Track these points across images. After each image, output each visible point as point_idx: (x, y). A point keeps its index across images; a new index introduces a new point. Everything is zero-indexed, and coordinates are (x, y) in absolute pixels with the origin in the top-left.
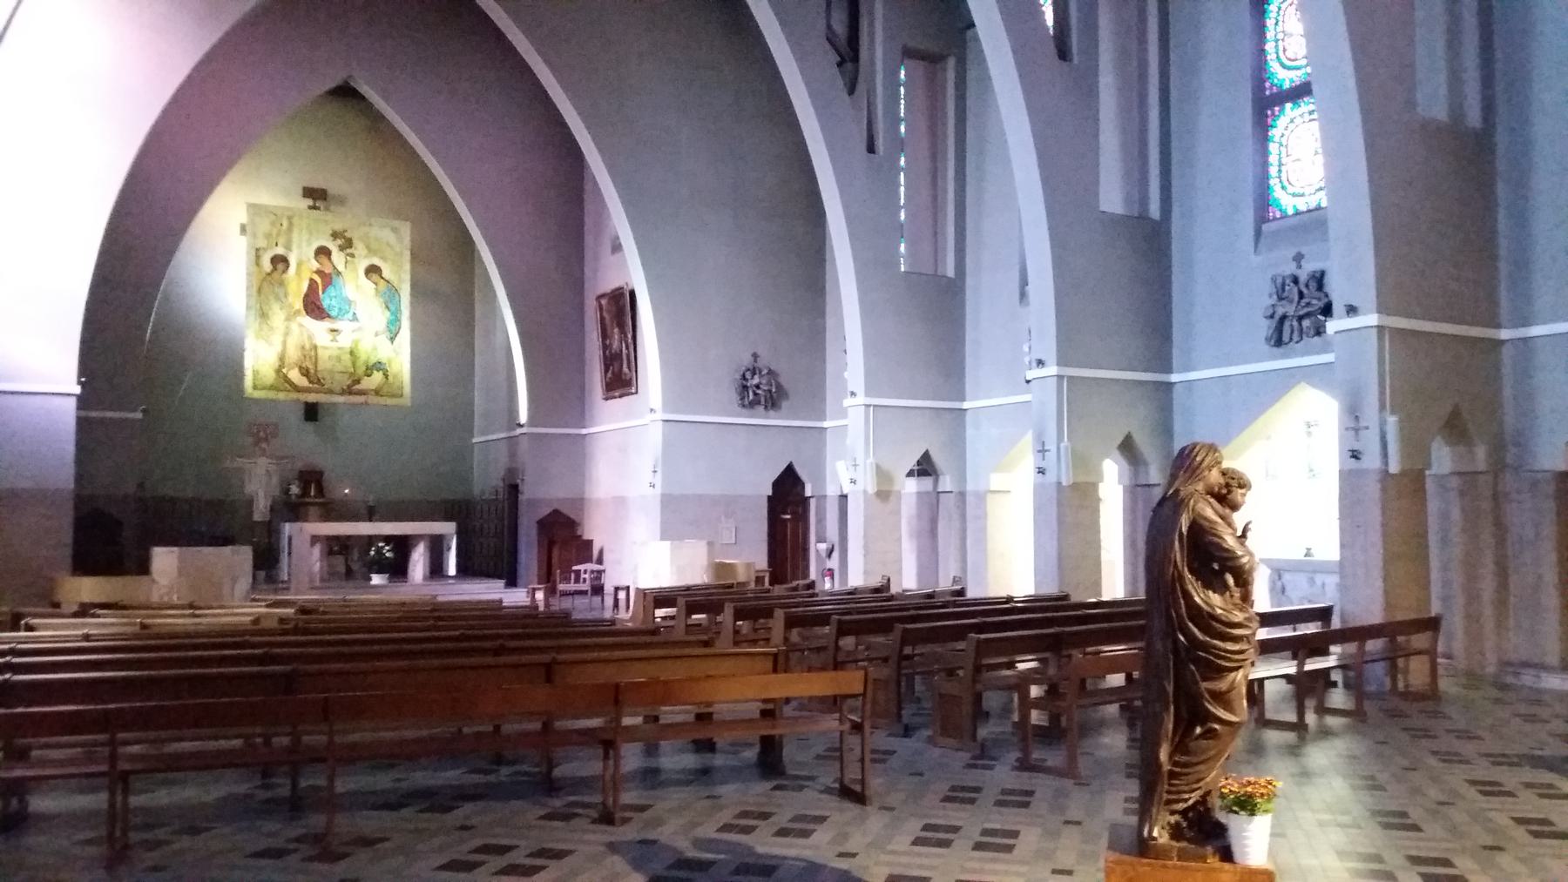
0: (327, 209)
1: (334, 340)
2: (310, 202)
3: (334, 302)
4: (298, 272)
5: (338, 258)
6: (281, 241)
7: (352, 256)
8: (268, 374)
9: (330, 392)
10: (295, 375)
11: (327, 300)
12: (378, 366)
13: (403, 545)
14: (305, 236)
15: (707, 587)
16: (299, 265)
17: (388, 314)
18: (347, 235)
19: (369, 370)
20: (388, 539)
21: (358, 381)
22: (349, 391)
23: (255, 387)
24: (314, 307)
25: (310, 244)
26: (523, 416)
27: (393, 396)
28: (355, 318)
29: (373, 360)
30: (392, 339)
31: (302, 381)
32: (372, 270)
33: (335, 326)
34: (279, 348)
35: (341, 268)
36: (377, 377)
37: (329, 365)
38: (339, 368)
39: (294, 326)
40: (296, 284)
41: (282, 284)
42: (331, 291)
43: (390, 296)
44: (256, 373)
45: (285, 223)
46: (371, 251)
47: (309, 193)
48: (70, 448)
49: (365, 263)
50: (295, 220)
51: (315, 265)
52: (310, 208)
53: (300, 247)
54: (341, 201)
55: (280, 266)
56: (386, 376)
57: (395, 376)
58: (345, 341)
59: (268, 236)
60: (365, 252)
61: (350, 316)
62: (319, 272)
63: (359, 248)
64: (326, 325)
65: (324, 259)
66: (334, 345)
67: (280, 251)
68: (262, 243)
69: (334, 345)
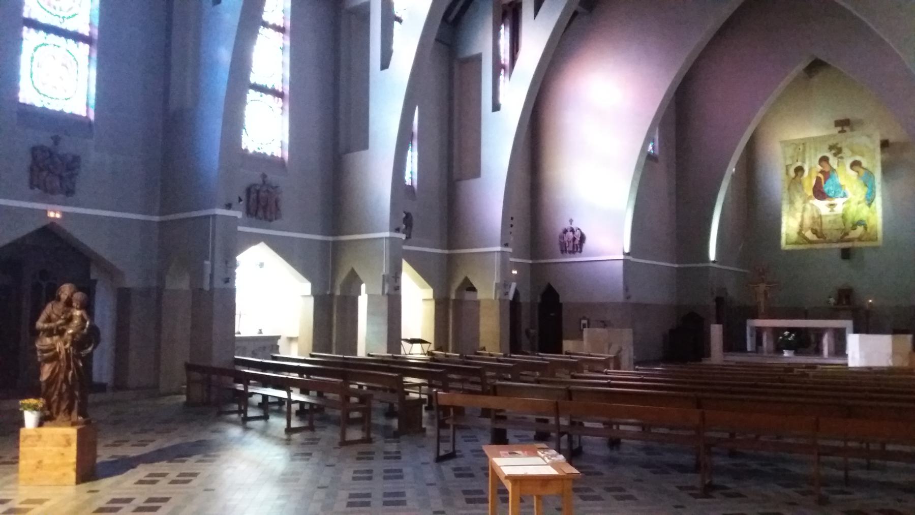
0: (852, 130)
1: (832, 211)
2: (839, 129)
3: (831, 188)
4: (810, 175)
5: (833, 162)
6: (800, 158)
7: (842, 158)
8: (794, 235)
9: (830, 242)
10: (809, 234)
11: (828, 187)
12: (861, 223)
13: (820, 332)
14: (813, 151)
15: (890, 371)
16: (810, 170)
17: (866, 189)
18: (839, 146)
19: (855, 226)
20: (791, 330)
21: (847, 234)
22: (842, 240)
23: (787, 243)
24: (819, 193)
25: (816, 155)
26: (712, 256)
27: (871, 240)
28: (845, 196)
29: (857, 219)
30: (869, 205)
31: (815, 238)
32: (855, 165)
33: (832, 202)
34: (799, 220)
35: (835, 167)
36: (860, 229)
37: (829, 227)
38: (837, 227)
39: (808, 206)
40: (808, 181)
41: (801, 183)
42: (830, 181)
43: (867, 180)
44: (787, 235)
45: (801, 147)
46: (854, 153)
47: (838, 123)
48: (621, 280)
49: (848, 162)
50: (808, 145)
51: (820, 168)
52: (840, 132)
53: (810, 160)
54: (860, 123)
55: (799, 173)
56: (866, 228)
57: (872, 227)
58: (839, 210)
59: (792, 157)
60: (850, 153)
61: (842, 195)
62: (822, 172)
63: (846, 152)
64: (827, 202)
65: (824, 163)
66: (832, 213)
67: (799, 164)
68: (789, 162)
69: (832, 213)
